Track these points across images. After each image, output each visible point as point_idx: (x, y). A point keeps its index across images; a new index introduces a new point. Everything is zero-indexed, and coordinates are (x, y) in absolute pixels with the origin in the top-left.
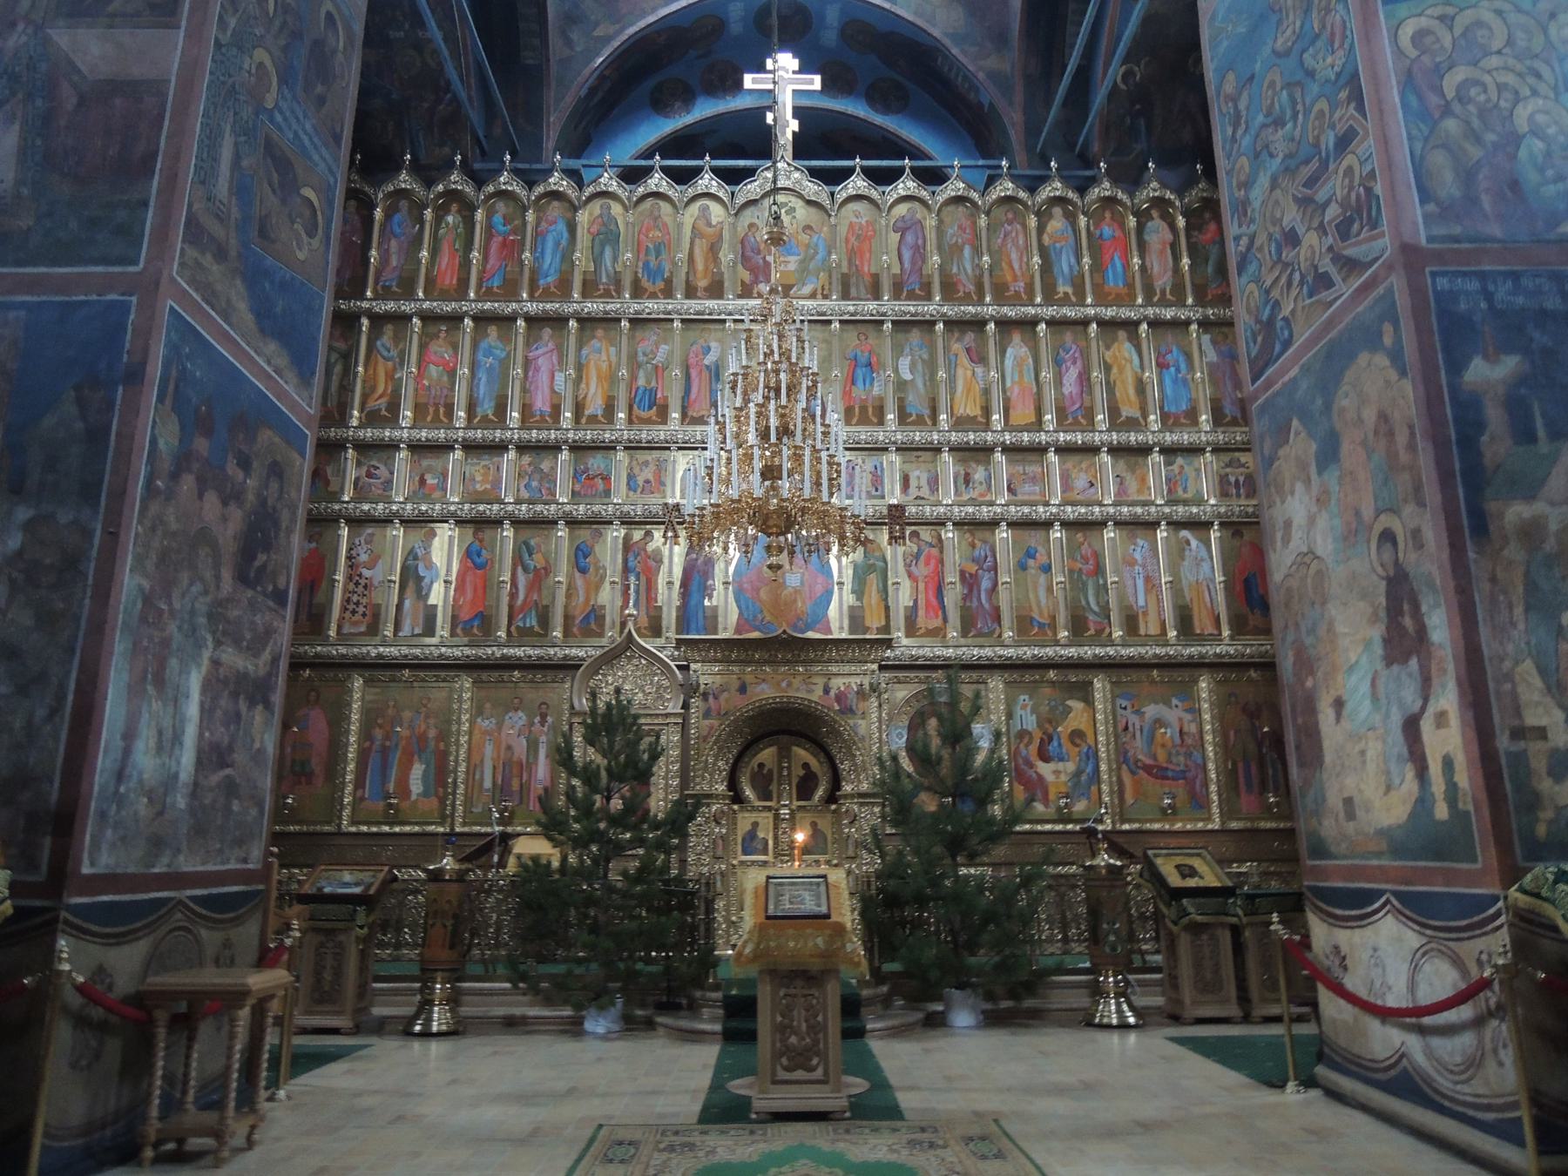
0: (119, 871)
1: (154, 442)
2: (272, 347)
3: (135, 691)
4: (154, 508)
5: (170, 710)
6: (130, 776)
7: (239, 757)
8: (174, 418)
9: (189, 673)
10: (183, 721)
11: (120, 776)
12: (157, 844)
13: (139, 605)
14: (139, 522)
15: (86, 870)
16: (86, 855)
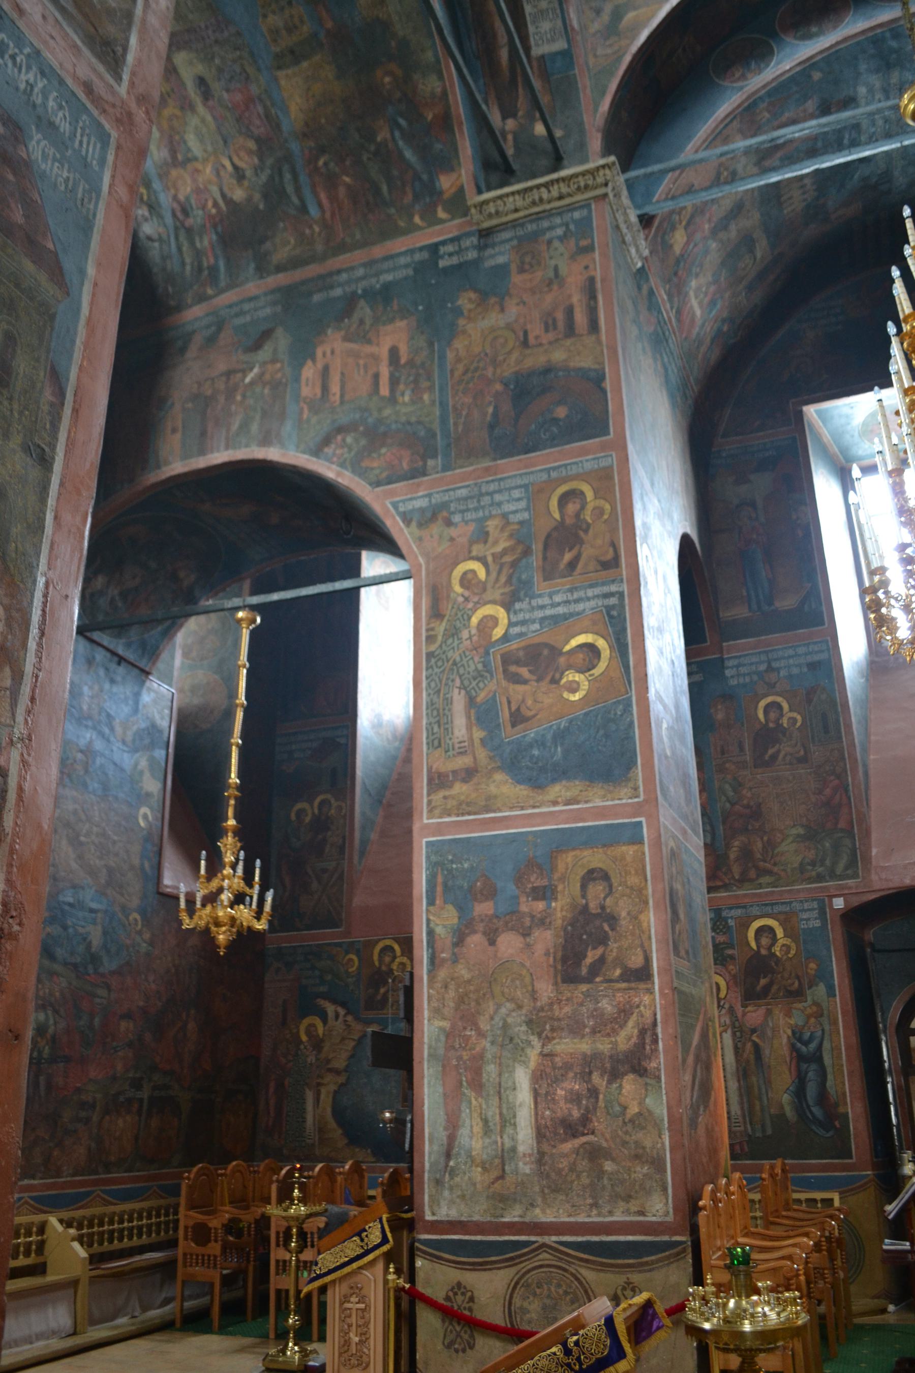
0: (463, 1219)
1: (431, 933)
2: (557, 790)
3: (453, 1099)
4: (442, 974)
5: (495, 1101)
6: (459, 1154)
7: (600, 1123)
8: (450, 907)
9: (512, 1072)
10: (512, 1109)
11: (448, 1156)
12: (503, 1200)
13: (443, 1038)
14: (430, 986)
15: (429, 1217)
16: (427, 1208)
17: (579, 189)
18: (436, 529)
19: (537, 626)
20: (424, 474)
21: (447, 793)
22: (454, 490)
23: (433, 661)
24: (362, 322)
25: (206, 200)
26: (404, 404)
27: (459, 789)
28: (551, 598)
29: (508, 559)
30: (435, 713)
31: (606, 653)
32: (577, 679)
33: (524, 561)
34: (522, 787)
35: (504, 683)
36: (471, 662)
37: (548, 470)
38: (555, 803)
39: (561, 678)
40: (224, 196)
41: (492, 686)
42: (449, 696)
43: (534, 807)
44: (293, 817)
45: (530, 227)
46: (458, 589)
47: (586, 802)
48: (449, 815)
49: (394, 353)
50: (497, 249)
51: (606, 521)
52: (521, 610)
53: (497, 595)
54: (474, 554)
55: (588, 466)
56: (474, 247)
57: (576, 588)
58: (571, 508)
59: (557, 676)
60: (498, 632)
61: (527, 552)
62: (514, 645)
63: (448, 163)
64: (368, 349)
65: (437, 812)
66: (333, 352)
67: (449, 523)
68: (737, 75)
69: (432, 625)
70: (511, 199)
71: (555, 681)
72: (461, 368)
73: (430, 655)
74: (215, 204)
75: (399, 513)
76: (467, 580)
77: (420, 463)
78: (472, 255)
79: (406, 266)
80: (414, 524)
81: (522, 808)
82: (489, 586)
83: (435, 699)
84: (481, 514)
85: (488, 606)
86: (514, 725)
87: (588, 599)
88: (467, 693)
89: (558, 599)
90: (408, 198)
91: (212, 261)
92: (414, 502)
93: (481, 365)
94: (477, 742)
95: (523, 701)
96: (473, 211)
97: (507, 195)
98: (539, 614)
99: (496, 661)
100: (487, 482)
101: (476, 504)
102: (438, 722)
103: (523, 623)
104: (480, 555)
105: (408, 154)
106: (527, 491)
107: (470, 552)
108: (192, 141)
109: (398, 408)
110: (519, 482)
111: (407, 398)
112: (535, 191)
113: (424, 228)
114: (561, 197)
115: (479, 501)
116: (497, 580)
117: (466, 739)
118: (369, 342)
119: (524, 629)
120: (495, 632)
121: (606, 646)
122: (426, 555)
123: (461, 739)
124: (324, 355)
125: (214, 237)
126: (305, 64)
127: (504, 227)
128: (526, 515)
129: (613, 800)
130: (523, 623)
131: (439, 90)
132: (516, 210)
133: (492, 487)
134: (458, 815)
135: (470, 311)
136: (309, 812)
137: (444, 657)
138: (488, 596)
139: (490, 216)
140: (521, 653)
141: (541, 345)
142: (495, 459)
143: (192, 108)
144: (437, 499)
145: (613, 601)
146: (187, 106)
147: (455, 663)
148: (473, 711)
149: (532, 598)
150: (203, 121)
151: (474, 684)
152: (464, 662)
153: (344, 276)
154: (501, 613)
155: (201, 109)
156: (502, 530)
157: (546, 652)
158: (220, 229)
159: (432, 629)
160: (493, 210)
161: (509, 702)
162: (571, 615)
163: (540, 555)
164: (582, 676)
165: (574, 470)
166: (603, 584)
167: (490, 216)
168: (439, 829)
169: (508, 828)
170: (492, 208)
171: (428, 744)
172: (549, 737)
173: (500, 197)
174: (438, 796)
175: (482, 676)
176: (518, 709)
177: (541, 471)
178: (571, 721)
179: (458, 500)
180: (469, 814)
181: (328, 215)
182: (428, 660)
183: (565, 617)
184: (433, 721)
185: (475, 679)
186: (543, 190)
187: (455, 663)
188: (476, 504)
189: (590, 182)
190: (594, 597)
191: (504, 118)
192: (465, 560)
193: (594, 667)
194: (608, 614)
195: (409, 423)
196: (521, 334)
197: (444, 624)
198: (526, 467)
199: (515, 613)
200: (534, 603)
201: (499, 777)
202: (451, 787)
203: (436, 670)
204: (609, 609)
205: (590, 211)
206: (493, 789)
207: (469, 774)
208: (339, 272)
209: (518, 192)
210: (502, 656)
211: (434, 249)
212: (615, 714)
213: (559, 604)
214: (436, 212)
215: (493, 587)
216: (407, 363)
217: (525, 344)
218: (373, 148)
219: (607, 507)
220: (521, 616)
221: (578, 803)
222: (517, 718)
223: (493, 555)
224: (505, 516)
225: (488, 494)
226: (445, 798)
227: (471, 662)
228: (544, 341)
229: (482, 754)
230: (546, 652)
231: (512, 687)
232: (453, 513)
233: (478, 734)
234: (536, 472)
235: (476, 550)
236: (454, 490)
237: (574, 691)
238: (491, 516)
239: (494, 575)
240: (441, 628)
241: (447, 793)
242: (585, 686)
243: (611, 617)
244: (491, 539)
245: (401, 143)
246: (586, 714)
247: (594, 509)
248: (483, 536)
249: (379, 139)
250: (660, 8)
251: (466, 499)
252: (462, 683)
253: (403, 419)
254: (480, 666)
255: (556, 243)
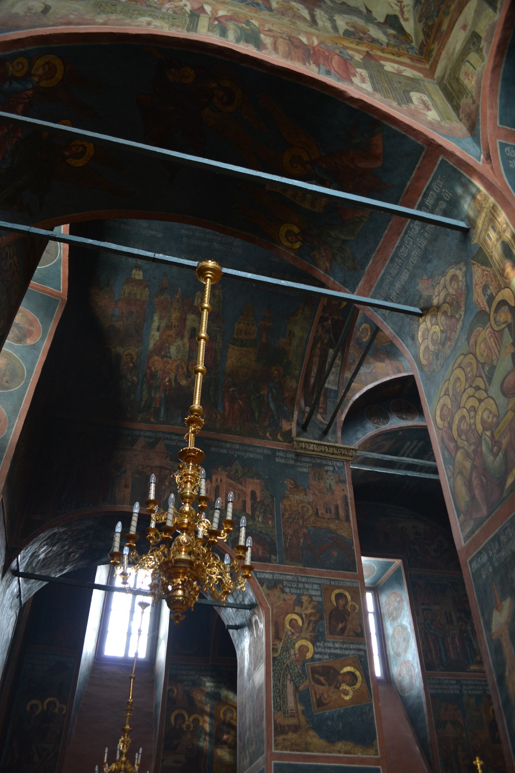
2: (340, 745)
17: (341, 454)
18: (277, 592)
19: (327, 657)
20: (270, 561)
21: (285, 737)
22: (285, 575)
23: (276, 662)
24: (237, 471)
25: (166, 377)
26: (259, 521)
27: (291, 736)
28: (334, 645)
29: (313, 618)
30: (278, 691)
31: (360, 679)
32: (347, 689)
33: (320, 621)
34: (323, 740)
35: (312, 683)
36: (296, 668)
37: (330, 580)
38: (340, 752)
39: (340, 687)
40: (176, 379)
41: (307, 683)
42: (285, 683)
43: (330, 752)
44: (28, 708)
45: (318, 461)
46: (288, 626)
47: (354, 754)
48: (286, 750)
49: (253, 493)
50: (302, 464)
51: (357, 613)
52: (319, 647)
53: (308, 636)
54: (296, 611)
55: (348, 584)
56: (293, 459)
57: (345, 642)
58: (341, 602)
59: (338, 685)
60: (309, 655)
61: (321, 618)
62: (317, 664)
63: (289, 417)
64: (240, 486)
65: (280, 747)
66: (221, 481)
67: (283, 592)
68: (376, 421)
69: (275, 643)
70: (312, 445)
71: (337, 688)
72: (287, 516)
73: (274, 659)
74: (170, 381)
75: (257, 578)
76: (292, 622)
77: (268, 556)
78: (291, 462)
79: (260, 454)
80: (265, 586)
81: (324, 752)
82: (304, 630)
83: (278, 683)
84: (299, 592)
85: (304, 640)
86: (318, 706)
87: (351, 649)
88: (295, 684)
89: (337, 645)
90: (266, 424)
91: (158, 406)
92: (265, 575)
93: (297, 517)
94: (300, 712)
95: (322, 694)
96: (295, 443)
97: (311, 443)
98: (328, 651)
99: (308, 671)
100: (302, 576)
101: (296, 586)
102: (279, 696)
103: (321, 653)
104: (299, 612)
105: (272, 405)
106: (320, 587)
107: (294, 609)
108: (173, 350)
109: (256, 523)
110: (316, 581)
111: (260, 520)
112: (323, 446)
113: (271, 440)
114: (333, 454)
115: (297, 585)
116: (308, 628)
117: (294, 708)
118: (241, 483)
119: (321, 657)
120: (307, 655)
121: (360, 675)
122: (272, 605)
123: (291, 708)
124: (217, 480)
125: (163, 395)
126: (244, 349)
127: (306, 455)
128: (320, 599)
129: (366, 755)
130: (321, 653)
131: (295, 387)
132: (313, 451)
133: (304, 580)
134: (291, 751)
135: (291, 488)
136: (40, 708)
137: (282, 661)
138: (303, 634)
139: (302, 448)
140: (320, 669)
141: (324, 518)
142: (305, 566)
143: (182, 337)
144: (276, 577)
145: (362, 653)
146: (180, 335)
147: (287, 666)
148: (297, 694)
149: (325, 641)
150: (184, 345)
151: (297, 680)
152: (292, 666)
153: (229, 445)
154: (310, 646)
155: (186, 340)
156: (310, 602)
157: (332, 671)
158: (167, 393)
159: (276, 645)
160: (304, 447)
161: (315, 694)
162: (343, 655)
163: (328, 621)
164: (349, 688)
165: (341, 584)
166: (357, 644)
167: (302, 448)
168: (281, 757)
169: (316, 762)
170: (303, 445)
171: (274, 707)
172: (335, 716)
173: (308, 443)
174: (280, 738)
175: (302, 676)
176: (320, 698)
177: (327, 579)
178: (345, 710)
179: (288, 581)
180: (297, 751)
181: (226, 413)
182: (274, 662)
183: (341, 656)
184: (277, 695)
185: (298, 677)
186: (326, 447)
187: (287, 666)
188: (296, 586)
189: (346, 453)
190: (353, 649)
191: (306, 405)
192: (291, 613)
193: (355, 684)
194: (360, 659)
195: (261, 532)
196: (315, 509)
197: (281, 643)
198: (319, 575)
199: (317, 647)
200: (326, 644)
201: (312, 733)
202: (287, 734)
203: (278, 667)
204: (361, 657)
205: (344, 465)
206: (309, 739)
207: (296, 729)
208: (226, 442)
209: (317, 444)
210: (312, 668)
211: (274, 451)
212: (366, 711)
213: (337, 648)
214: (277, 436)
215: (306, 631)
216: (260, 502)
217: (317, 514)
218: (257, 395)
219: (357, 606)
220: (320, 650)
221: (350, 753)
222: (320, 703)
223: (305, 614)
224: (310, 596)
225: (302, 582)
226: (284, 739)
227: (296, 668)
228: (326, 517)
229: (303, 719)
230: (332, 671)
231: (317, 686)
232: (286, 587)
233: (301, 708)
234: (324, 579)
235: (297, 609)
236: (285, 575)
237: (347, 694)
238: (303, 594)
239: (306, 625)
240: (280, 645)
241: (285, 737)
242: (351, 693)
243: (361, 661)
244: (304, 605)
245: (270, 399)
246: (353, 708)
247: (352, 606)
248: (299, 602)
249: (261, 393)
250: (364, 387)
251: (291, 581)
252: (291, 677)
253: (259, 530)
254: (300, 671)
255: (330, 473)
